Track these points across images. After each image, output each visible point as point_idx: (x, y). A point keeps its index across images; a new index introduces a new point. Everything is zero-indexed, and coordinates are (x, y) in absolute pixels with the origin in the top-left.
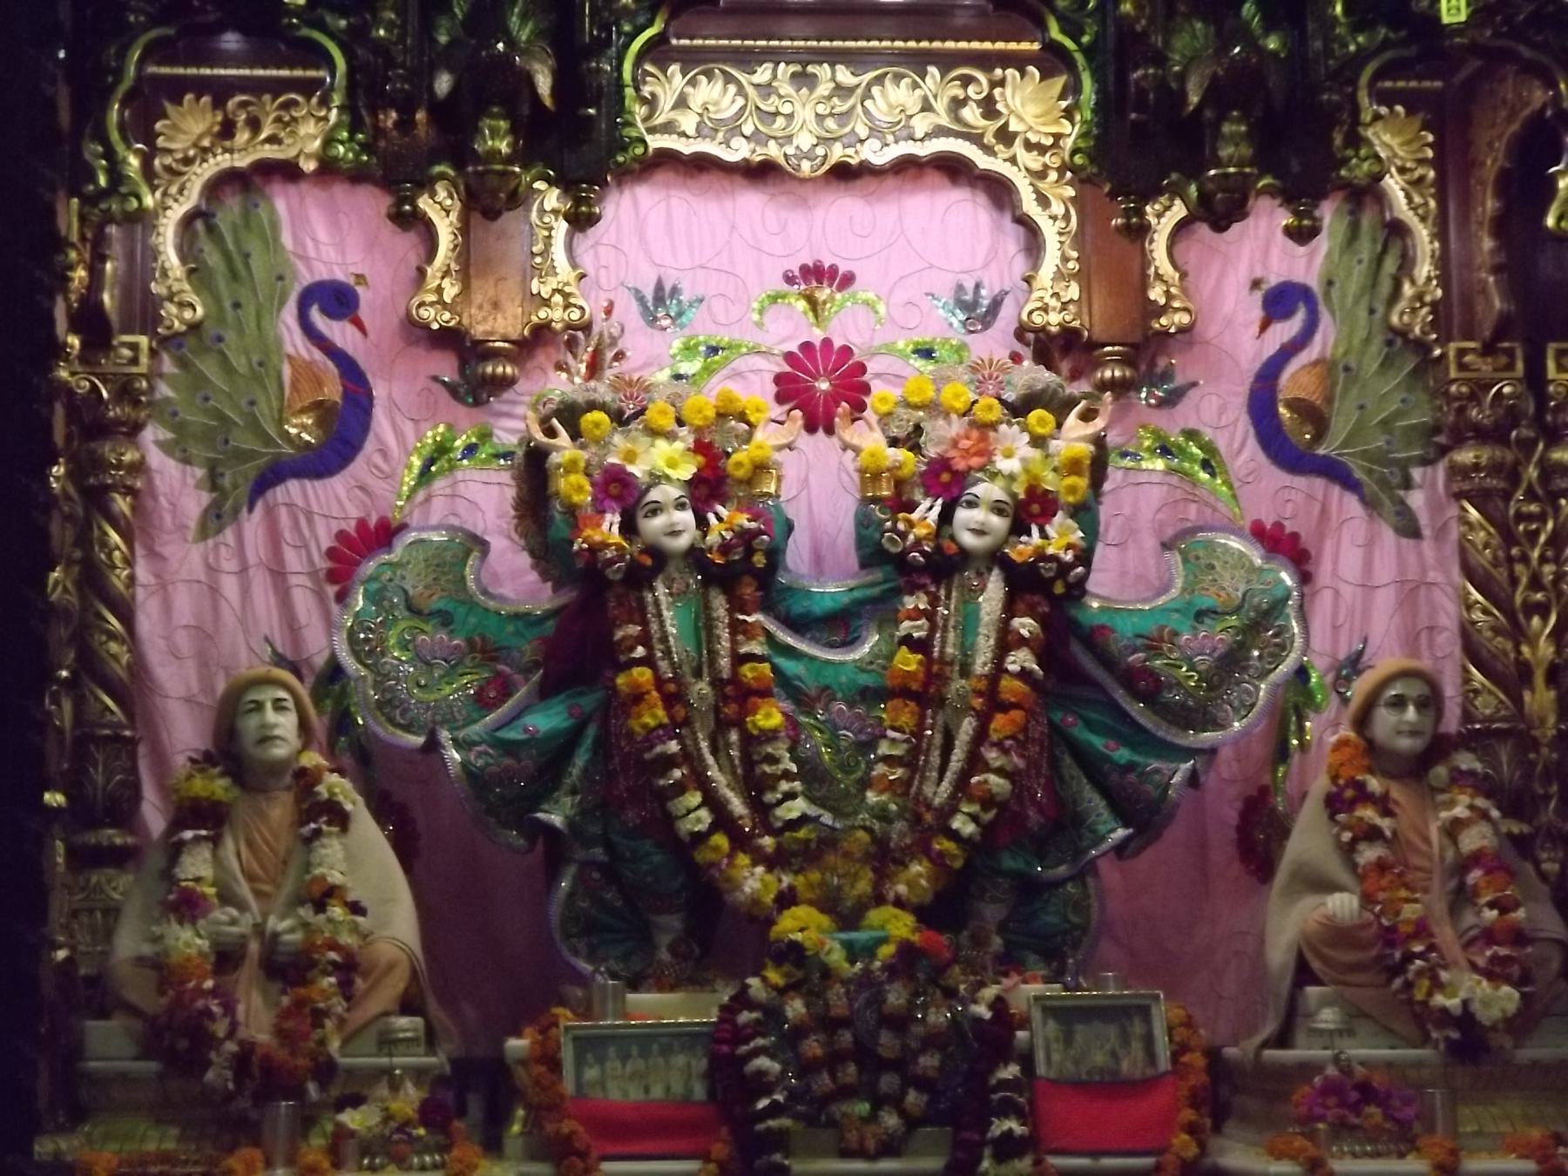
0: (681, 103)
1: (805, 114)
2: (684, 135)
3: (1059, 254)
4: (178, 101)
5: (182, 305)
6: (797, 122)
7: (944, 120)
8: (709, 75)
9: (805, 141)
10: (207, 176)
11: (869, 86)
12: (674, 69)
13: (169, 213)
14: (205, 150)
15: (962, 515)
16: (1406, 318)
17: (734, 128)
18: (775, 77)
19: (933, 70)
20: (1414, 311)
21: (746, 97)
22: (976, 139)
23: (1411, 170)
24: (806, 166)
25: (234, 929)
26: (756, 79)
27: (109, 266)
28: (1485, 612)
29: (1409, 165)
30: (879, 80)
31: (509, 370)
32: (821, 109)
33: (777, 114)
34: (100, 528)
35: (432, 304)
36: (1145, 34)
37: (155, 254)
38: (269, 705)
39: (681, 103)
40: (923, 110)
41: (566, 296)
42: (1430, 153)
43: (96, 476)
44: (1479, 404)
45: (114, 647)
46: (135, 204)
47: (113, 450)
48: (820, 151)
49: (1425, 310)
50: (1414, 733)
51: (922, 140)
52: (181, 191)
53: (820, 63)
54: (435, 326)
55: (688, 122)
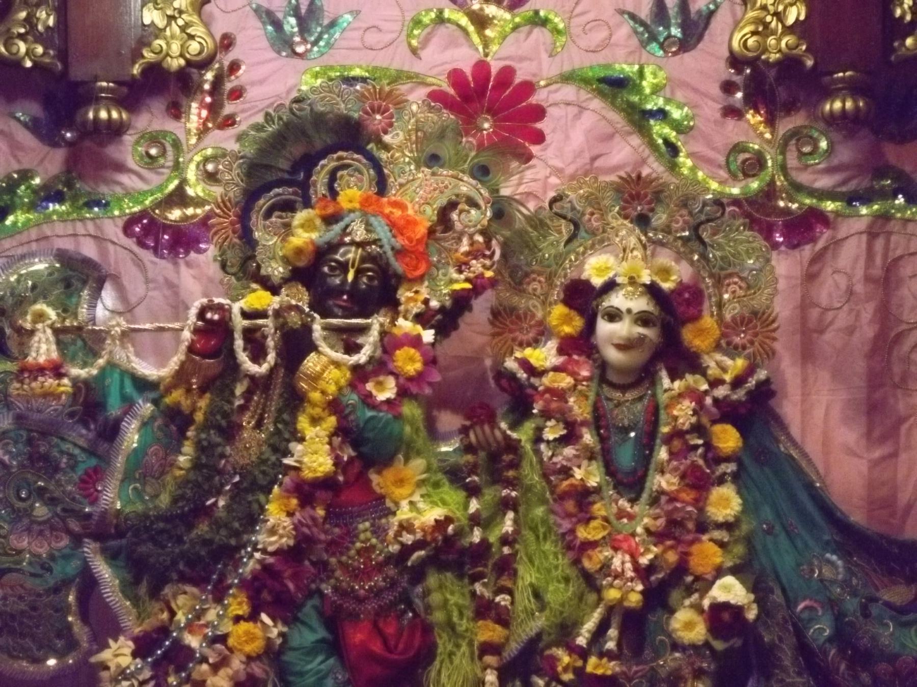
31: (115, 115)
54: (29, 64)
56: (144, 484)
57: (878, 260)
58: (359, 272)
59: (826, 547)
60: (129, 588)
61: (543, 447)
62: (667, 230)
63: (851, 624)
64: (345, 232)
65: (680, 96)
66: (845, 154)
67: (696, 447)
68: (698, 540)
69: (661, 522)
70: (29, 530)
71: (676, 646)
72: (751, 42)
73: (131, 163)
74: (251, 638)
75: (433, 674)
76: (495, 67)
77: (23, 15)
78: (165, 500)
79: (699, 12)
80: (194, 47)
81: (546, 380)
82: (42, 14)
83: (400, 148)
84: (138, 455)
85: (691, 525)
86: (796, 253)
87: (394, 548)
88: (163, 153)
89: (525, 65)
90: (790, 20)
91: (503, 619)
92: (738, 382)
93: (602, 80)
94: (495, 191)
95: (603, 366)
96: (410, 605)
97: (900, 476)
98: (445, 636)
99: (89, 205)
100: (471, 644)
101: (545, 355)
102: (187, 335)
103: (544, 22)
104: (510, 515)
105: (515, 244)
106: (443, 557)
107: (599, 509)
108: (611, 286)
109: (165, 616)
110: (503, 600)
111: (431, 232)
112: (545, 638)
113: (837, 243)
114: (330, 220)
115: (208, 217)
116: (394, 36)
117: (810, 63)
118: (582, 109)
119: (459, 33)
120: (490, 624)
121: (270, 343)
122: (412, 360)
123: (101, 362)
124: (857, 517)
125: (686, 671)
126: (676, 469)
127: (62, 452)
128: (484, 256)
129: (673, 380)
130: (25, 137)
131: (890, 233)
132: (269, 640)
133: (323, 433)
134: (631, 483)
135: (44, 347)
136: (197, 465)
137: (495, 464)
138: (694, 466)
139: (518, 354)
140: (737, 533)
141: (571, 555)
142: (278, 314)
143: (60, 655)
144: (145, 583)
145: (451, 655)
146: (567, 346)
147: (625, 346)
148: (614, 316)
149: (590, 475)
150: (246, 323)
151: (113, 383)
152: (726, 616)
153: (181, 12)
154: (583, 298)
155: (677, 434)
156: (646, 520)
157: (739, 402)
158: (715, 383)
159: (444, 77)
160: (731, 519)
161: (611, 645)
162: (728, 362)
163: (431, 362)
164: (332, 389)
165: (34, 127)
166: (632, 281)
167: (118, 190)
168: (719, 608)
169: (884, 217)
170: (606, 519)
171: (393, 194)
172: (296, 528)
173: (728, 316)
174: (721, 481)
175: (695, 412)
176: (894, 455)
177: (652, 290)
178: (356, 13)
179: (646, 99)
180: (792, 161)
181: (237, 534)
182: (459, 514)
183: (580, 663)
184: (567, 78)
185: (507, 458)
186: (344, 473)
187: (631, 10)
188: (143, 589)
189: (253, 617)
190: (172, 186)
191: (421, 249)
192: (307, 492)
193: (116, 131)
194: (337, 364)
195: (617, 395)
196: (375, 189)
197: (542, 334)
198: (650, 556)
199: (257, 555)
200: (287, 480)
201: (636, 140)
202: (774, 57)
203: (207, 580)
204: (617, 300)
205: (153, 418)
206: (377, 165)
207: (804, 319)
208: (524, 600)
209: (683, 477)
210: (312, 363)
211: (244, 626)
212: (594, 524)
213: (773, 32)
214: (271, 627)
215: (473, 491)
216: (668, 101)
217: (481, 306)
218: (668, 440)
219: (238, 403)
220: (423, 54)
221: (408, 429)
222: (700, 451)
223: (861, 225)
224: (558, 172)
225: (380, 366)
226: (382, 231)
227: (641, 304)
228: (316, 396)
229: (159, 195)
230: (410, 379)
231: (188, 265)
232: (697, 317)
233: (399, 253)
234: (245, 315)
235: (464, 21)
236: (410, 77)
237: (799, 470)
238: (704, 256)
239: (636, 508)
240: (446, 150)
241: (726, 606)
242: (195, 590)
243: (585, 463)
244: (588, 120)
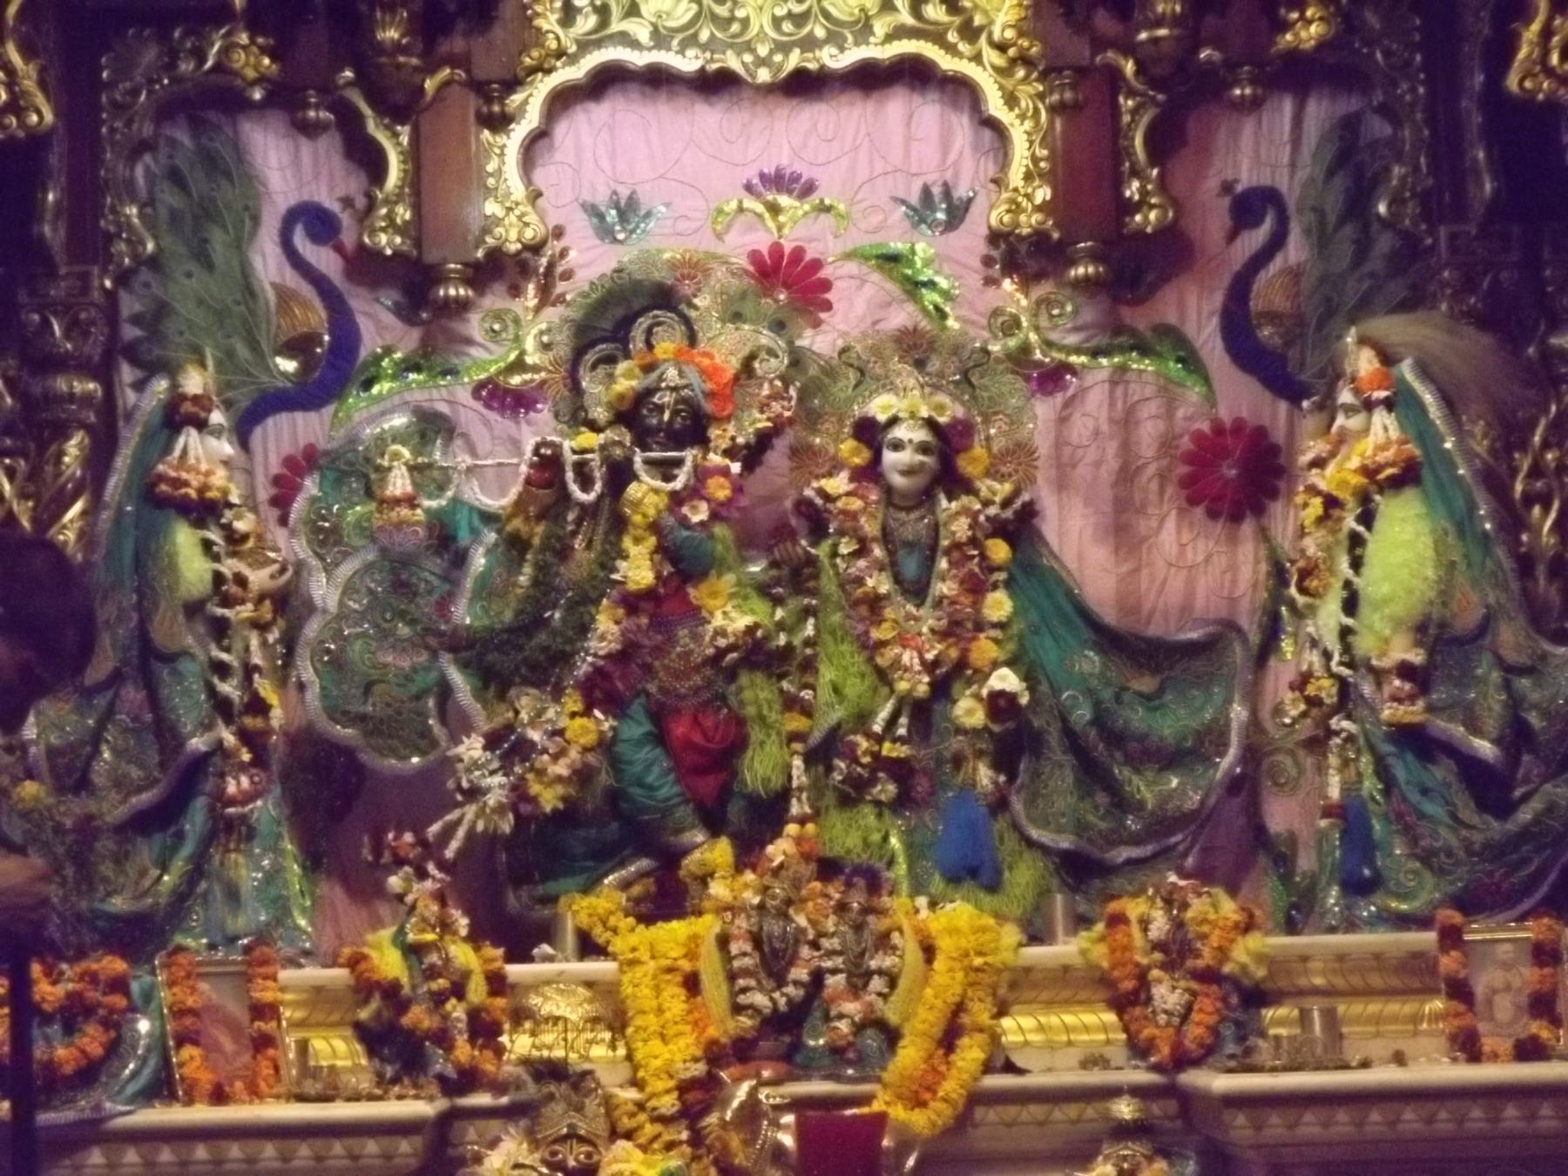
3: (1027, 154)
6: (754, 30)
7: (907, 19)
21: (700, 4)
22: (938, 37)
31: (462, 292)
32: (780, 11)
33: (732, 19)
46: (34, 118)
48: (778, 58)
54: (389, 252)
55: (642, 33)
56: (490, 603)
57: (1120, 405)
58: (675, 413)
59: (1084, 644)
60: (479, 694)
61: (838, 561)
62: (941, 375)
63: (1107, 710)
64: (660, 379)
65: (946, 269)
66: (1088, 315)
67: (973, 557)
68: (975, 639)
69: (944, 622)
70: (393, 647)
71: (960, 730)
72: (1006, 219)
73: (477, 334)
74: (585, 731)
75: (747, 762)
76: (788, 247)
77: (384, 211)
78: (508, 616)
79: (960, 199)
80: (529, 234)
81: (840, 504)
82: (400, 209)
83: (707, 309)
84: (484, 580)
85: (969, 625)
86: (1050, 400)
87: (710, 651)
88: (505, 329)
89: (814, 244)
90: (1038, 200)
91: (807, 711)
92: (1006, 503)
93: (878, 257)
94: (790, 343)
95: (889, 491)
96: (723, 698)
97: (1144, 586)
98: (757, 728)
99: (444, 373)
100: (779, 734)
101: (838, 484)
102: (524, 469)
103: (828, 209)
104: (811, 621)
105: (810, 383)
106: (754, 658)
107: (889, 613)
108: (894, 421)
109: (511, 714)
110: (806, 694)
111: (736, 378)
112: (844, 726)
113: (1083, 391)
114: (648, 368)
115: (543, 382)
116: (699, 223)
117: (1056, 235)
118: (864, 281)
119: (755, 219)
120: (795, 715)
121: (597, 474)
122: (722, 487)
123: (450, 494)
124: (1109, 616)
125: (968, 752)
126: (955, 576)
127: (420, 579)
128: (783, 398)
129: (950, 500)
130: (389, 319)
131: (1128, 382)
132: (601, 733)
133: (645, 551)
134: (917, 590)
135: (399, 482)
136: (536, 583)
137: (796, 578)
138: (972, 574)
139: (815, 484)
140: (1010, 632)
141: (866, 654)
142: (603, 448)
143: (422, 753)
144: (492, 688)
145: (762, 744)
146: (859, 475)
147: (908, 472)
148: (897, 446)
149: (881, 583)
150: (576, 457)
151: (462, 519)
152: (1002, 702)
153: (517, 204)
154: (870, 433)
155: (957, 546)
156: (930, 622)
157: (1007, 521)
158: (987, 503)
159: (744, 257)
160: (1004, 619)
161: (902, 731)
162: (997, 486)
163: (738, 490)
164: (652, 512)
165: (398, 311)
166: (913, 415)
167: (468, 362)
168: (996, 696)
169: (1123, 369)
170: (895, 621)
171: (702, 346)
172: (623, 634)
173: (995, 449)
174: (995, 587)
175: (971, 527)
176: (1137, 570)
177: (930, 424)
178: (667, 205)
179: (919, 272)
180: (1044, 322)
181: (571, 641)
182: (766, 622)
183: (876, 748)
184: (849, 256)
185: (807, 571)
186: (665, 585)
187: (901, 195)
188: (491, 693)
189: (587, 712)
190: (512, 356)
191: (728, 391)
192: (632, 602)
193: (463, 306)
194: (656, 491)
195: (903, 515)
196: (686, 342)
197: (834, 468)
198: (935, 652)
199: (590, 659)
200: (614, 593)
201: (910, 307)
202: (1026, 231)
203: (546, 683)
204: (900, 432)
205: (496, 545)
206: (687, 321)
207: (1058, 458)
208: (825, 694)
209: (962, 583)
210: (634, 491)
211: (579, 721)
212: (885, 625)
213: (1024, 211)
214: (603, 722)
215: (777, 601)
216: (937, 273)
217: (781, 445)
218: (947, 552)
219: (570, 528)
220: (729, 238)
221: (720, 547)
222: (976, 560)
223: (1103, 375)
224: (844, 334)
225: (694, 491)
226: (693, 377)
227: (921, 435)
228: (638, 519)
229: (502, 365)
230: (722, 504)
231: (529, 423)
232: (967, 448)
233: (710, 395)
234: (574, 452)
235: (760, 208)
236: (715, 257)
237: (1060, 581)
238: (974, 398)
239: (922, 612)
240: (748, 308)
241: (1002, 693)
242: (533, 691)
243: (876, 573)
244: (869, 290)
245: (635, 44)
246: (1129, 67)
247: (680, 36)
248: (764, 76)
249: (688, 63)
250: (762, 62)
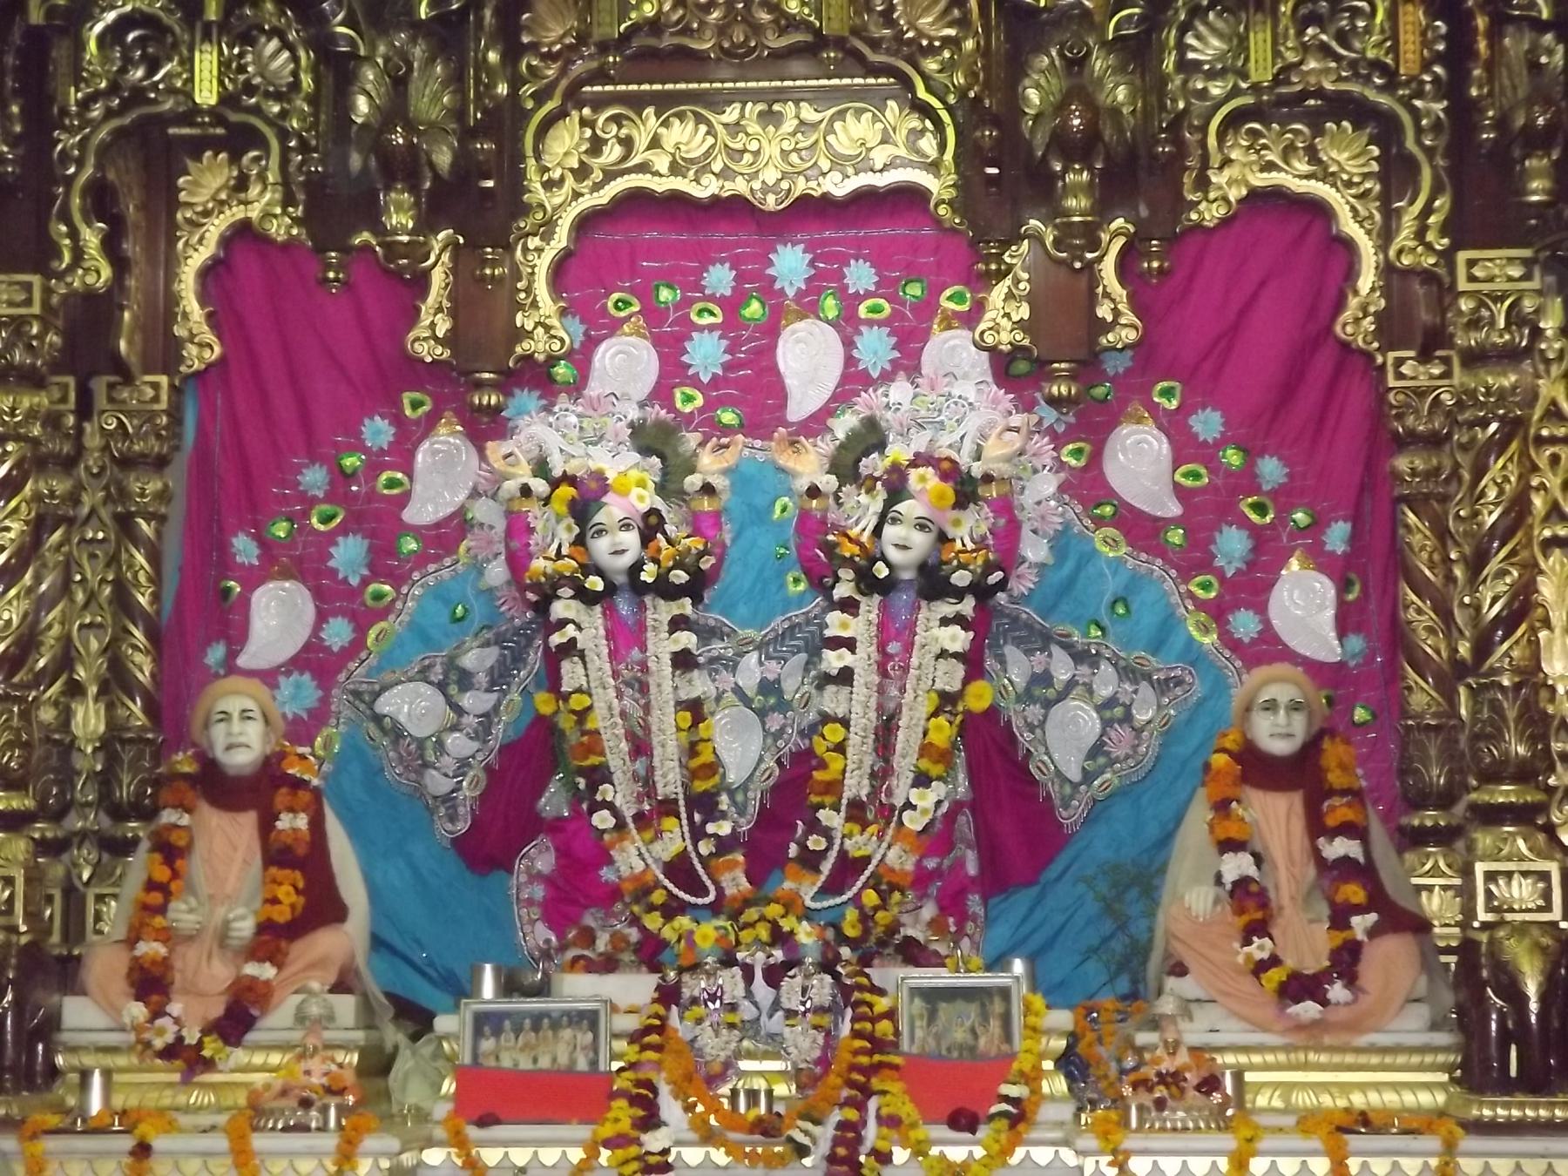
0: (655, 143)
1: (772, 150)
2: (657, 174)
4: (198, 158)
5: (201, 345)
6: (764, 158)
7: (902, 152)
8: (681, 116)
9: (770, 175)
10: (223, 228)
11: (832, 120)
12: (650, 111)
13: (189, 261)
14: (222, 203)
15: (889, 531)
16: (1349, 329)
17: (706, 169)
18: (742, 116)
19: (891, 104)
20: (1357, 321)
21: (715, 137)
23: (1358, 184)
24: (771, 199)
25: (191, 917)
26: (725, 118)
27: (127, 315)
28: (1419, 611)
29: (1356, 179)
30: (841, 115)
32: (786, 146)
33: (745, 150)
34: (127, 550)
35: (425, 339)
36: (978, 99)
37: (173, 300)
38: (236, 715)
39: (655, 143)
40: (883, 142)
41: (547, 328)
42: (1375, 167)
43: (123, 504)
44: (1417, 412)
45: (139, 658)
47: (137, 480)
49: (1370, 319)
50: (1289, 735)
51: (881, 171)
52: (200, 241)
53: (785, 101)
54: (429, 359)
55: (662, 163)
77: (427, 322)
245: (657, 174)
246: (1049, 240)
247: (695, 168)
248: (771, 203)
249: (705, 189)
250: (766, 189)
